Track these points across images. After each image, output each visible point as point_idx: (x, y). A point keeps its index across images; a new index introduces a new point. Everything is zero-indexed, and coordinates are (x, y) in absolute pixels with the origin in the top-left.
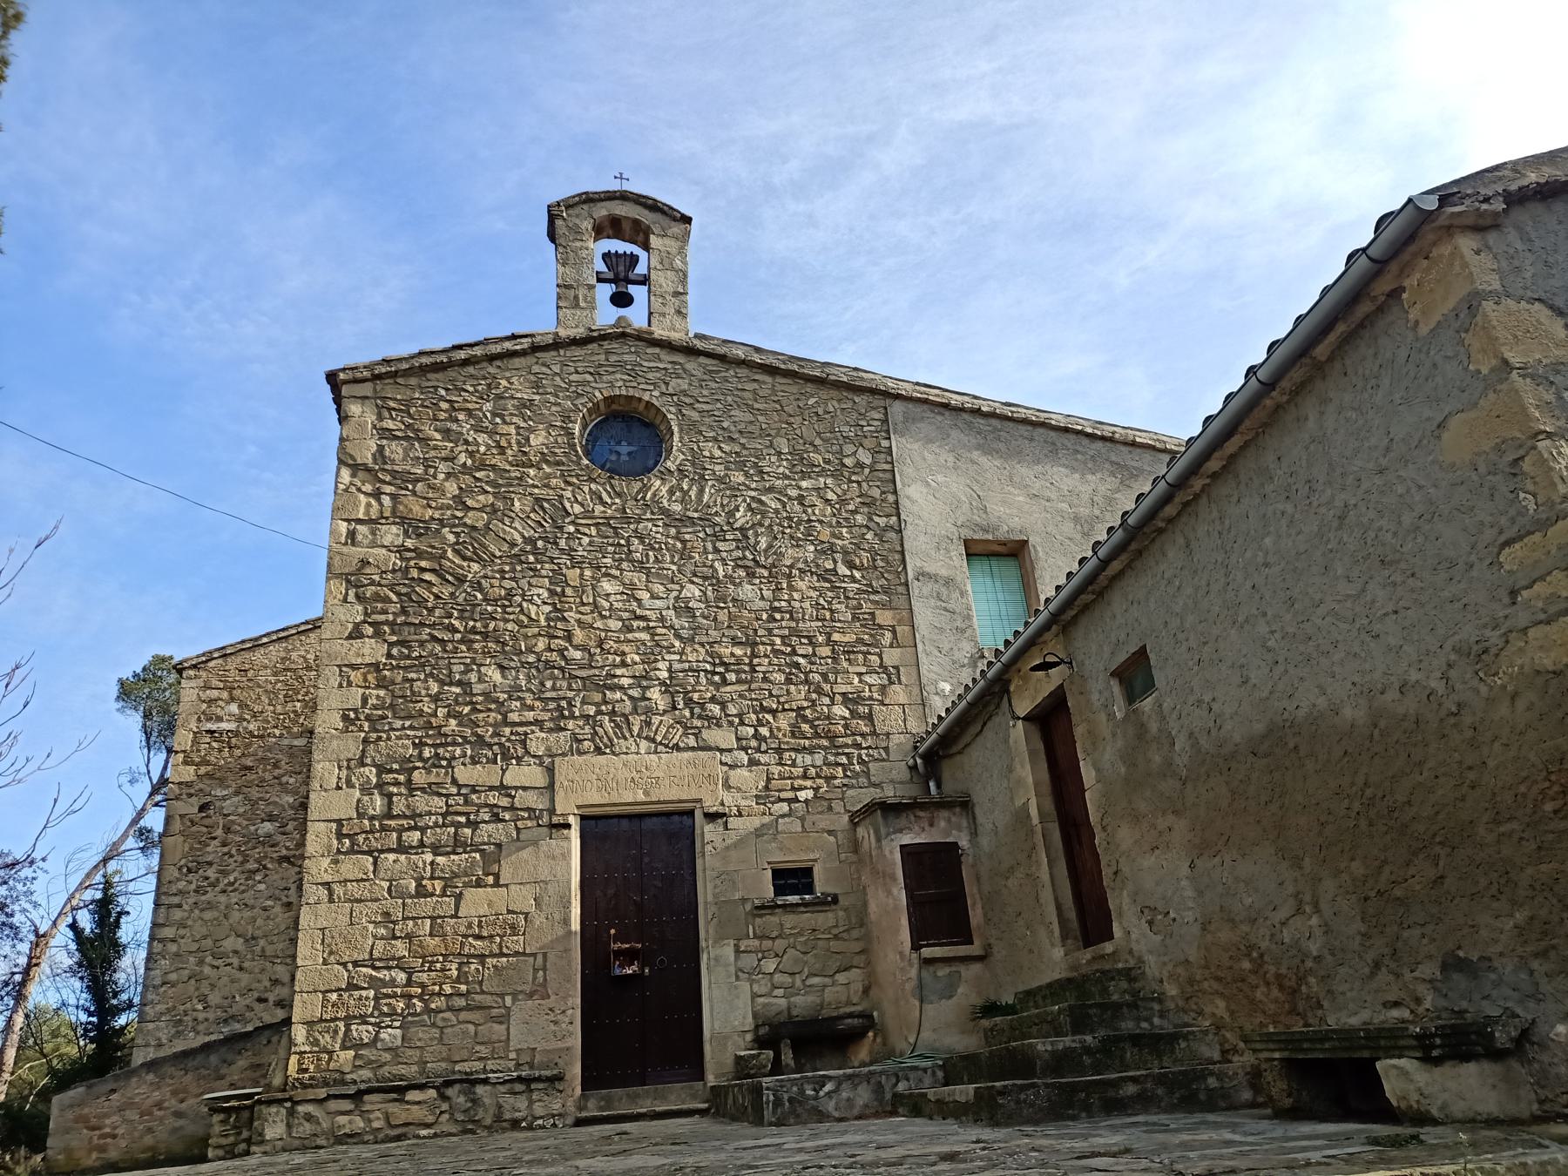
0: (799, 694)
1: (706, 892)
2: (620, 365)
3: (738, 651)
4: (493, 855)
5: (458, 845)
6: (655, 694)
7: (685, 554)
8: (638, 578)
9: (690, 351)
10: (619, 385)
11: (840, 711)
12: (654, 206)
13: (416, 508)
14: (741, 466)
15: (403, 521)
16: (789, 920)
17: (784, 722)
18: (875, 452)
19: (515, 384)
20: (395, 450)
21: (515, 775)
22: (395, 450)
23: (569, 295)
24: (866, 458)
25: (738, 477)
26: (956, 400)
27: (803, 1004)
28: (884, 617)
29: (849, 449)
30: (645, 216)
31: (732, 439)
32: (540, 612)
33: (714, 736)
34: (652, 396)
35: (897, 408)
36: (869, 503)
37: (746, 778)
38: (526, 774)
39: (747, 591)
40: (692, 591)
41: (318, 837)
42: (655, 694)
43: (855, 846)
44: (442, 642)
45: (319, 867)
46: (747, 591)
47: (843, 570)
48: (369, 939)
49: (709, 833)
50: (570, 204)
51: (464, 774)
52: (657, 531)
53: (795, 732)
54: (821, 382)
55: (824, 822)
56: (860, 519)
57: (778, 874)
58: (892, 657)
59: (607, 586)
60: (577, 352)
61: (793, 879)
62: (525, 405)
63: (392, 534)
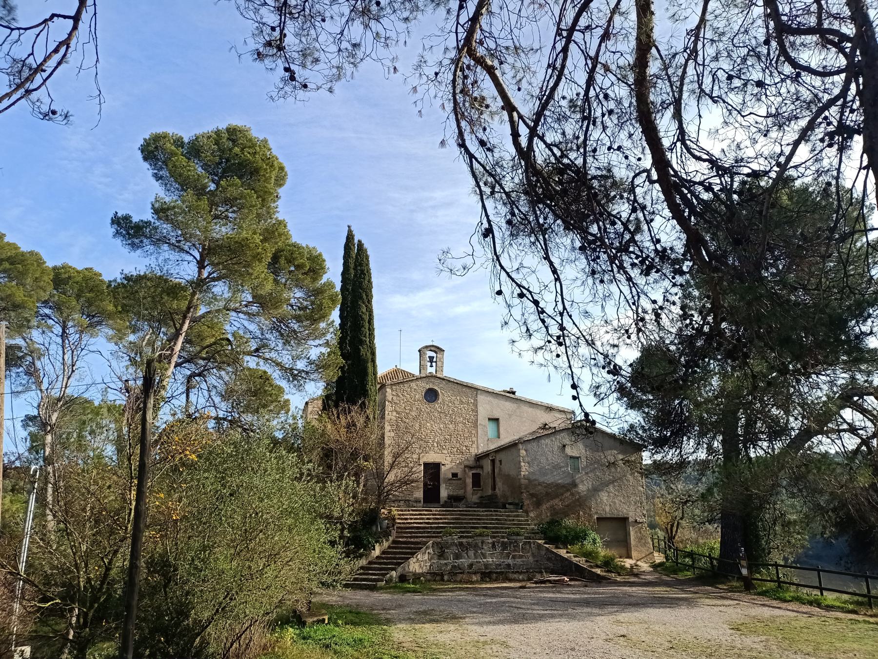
0: (458, 445)
1: (442, 476)
2: (431, 382)
6: (435, 444)
7: (441, 419)
8: (433, 423)
9: (443, 379)
11: (464, 448)
12: (438, 348)
13: (398, 409)
14: (451, 402)
16: (454, 482)
17: (455, 450)
18: (474, 400)
19: (413, 385)
20: (395, 398)
22: (395, 398)
23: (422, 367)
24: (472, 401)
25: (450, 404)
26: (490, 390)
27: (455, 494)
28: (473, 432)
30: (436, 350)
33: (444, 451)
35: (479, 392)
39: (451, 426)
40: (442, 426)
42: (435, 444)
43: (465, 471)
46: (451, 426)
49: (443, 468)
50: (424, 348)
53: (457, 452)
55: (460, 466)
58: (474, 439)
59: (428, 424)
61: (455, 475)
62: (415, 389)
63: (394, 414)
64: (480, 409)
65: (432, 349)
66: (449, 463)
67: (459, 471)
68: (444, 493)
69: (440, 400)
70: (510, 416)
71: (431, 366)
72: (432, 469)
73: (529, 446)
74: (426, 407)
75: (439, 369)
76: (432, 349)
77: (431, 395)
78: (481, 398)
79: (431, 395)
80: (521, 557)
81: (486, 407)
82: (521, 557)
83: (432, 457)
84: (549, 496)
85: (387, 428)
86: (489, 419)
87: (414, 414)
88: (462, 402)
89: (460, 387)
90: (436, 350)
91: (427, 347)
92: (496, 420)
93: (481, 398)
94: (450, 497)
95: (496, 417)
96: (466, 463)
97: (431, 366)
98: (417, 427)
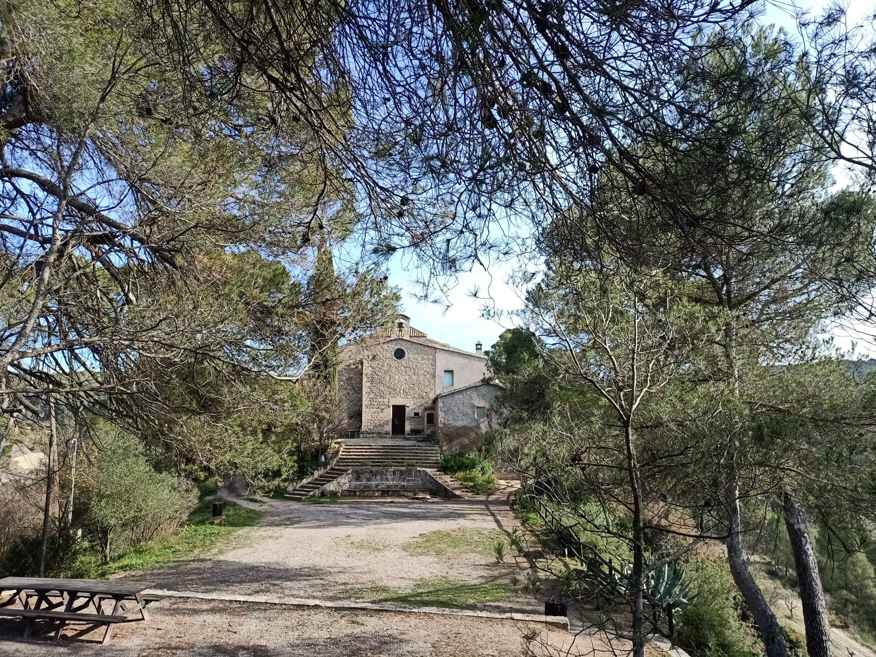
4: (382, 410)
32: (388, 380)
37: (412, 402)
38: (386, 400)
41: (364, 406)
45: (364, 409)
48: (370, 418)
49: (407, 409)
52: (403, 368)
61: (416, 414)
64: (438, 363)
66: (412, 406)
67: (420, 411)
68: (408, 427)
69: (406, 357)
70: (462, 368)
72: (399, 411)
73: (445, 400)
74: (395, 362)
77: (400, 354)
78: (439, 356)
79: (400, 354)
80: (413, 480)
81: (443, 361)
82: (413, 480)
83: (399, 401)
84: (459, 436)
85: (365, 379)
87: (385, 368)
88: (423, 359)
89: (422, 347)
92: (452, 372)
93: (439, 356)
94: (414, 432)
96: (426, 405)
98: (388, 379)
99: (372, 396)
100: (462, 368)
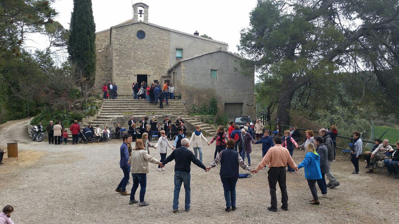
3: (152, 60)
5: (126, 77)
9: (148, 25)
10: (140, 29)
15: (119, 44)
21: (131, 71)
29: (165, 37)
30: (144, 6)
31: (152, 36)
34: (144, 30)
35: (171, 32)
36: (167, 44)
41: (114, 75)
44: (124, 57)
47: (163, 51)
51: (127, 70)
54: (162, 29)
56: (165, 45)
57: (154, 81)
60: (136, 25)
65: (141, 5)
71: (141, 16)
74: (138, 41)
75: (146, 18)
76: (141, 5)
79: (141, 35)
81: (175, 42)
86: (177, 49)
89: (158, 30)
90: (144, 6)
91: (137, 4)
93: (173, 35)
95: (181, 48)
97: (141, 16)
99: (121, 67)
100: (189, 47)
